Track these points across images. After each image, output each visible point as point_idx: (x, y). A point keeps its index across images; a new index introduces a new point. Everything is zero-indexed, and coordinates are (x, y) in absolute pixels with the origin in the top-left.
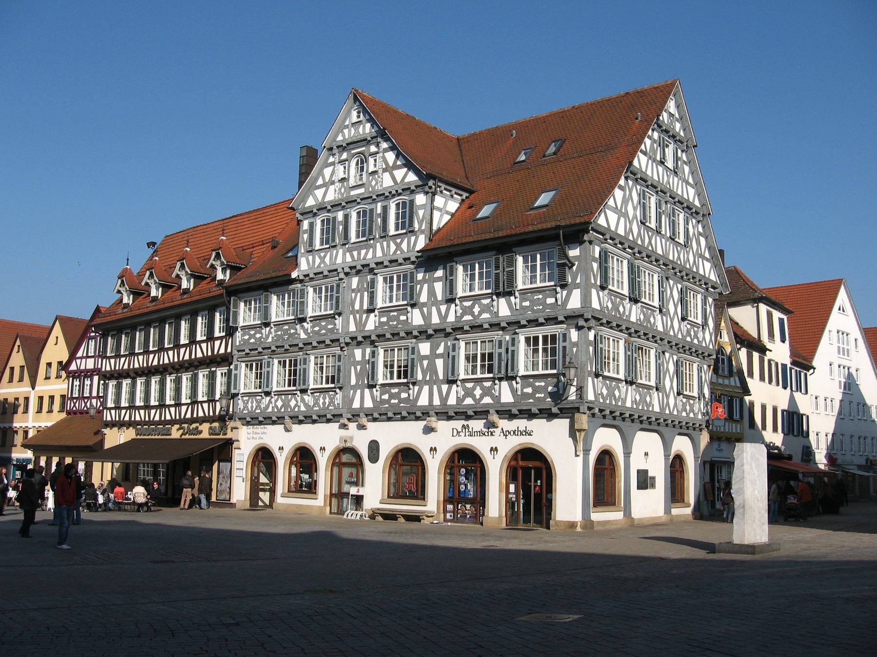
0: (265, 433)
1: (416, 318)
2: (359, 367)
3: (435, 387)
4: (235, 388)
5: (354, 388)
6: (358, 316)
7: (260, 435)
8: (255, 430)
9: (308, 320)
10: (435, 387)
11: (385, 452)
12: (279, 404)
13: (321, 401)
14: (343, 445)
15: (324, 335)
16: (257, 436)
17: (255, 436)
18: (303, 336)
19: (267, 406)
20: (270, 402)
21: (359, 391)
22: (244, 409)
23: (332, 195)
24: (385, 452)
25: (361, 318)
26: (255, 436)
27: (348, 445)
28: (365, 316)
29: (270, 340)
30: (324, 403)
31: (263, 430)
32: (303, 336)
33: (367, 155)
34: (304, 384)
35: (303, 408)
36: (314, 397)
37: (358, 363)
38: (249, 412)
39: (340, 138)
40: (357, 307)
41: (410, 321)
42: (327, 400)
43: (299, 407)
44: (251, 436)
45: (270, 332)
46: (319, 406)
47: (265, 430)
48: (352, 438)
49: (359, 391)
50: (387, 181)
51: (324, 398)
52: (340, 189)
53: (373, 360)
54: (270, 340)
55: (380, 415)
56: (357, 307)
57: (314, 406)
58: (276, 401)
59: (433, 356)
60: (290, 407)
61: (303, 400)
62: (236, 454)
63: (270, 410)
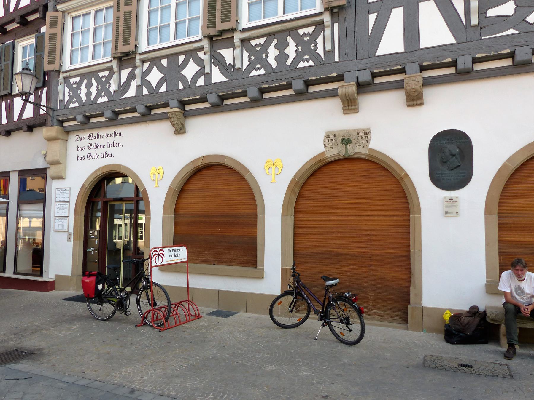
0: (115, 145)
4: (52, 61)
7: (109, 151)
8: (94, 142)
11: (488, 163)
12: (155, 76)
13: (273, 52)
14: (335, 152)
16: (100, 152)
17: (93, 152)
19: (126, 87)
20: (131, 77)
22: (70, 101)
24: (488, 163)
26: (93, 152)
27: (356, 149)
30: (282, 58)
31: (111, 140)
34: (226, 18)
35: (218, 77)
36: (251, 50)
38: (82, 105)
42: (291, 50)
43: (209, 76)
44: (84, 153)
46: (266, 65)
47: (117, 139)
48: (365, 135)
51: (282, 46)
55: (458, 67)
57: (251, 67)
58: (145, 74)
60: (184, 79)
61: (218, 61)
62: (54, 189)
63: (131, 92)
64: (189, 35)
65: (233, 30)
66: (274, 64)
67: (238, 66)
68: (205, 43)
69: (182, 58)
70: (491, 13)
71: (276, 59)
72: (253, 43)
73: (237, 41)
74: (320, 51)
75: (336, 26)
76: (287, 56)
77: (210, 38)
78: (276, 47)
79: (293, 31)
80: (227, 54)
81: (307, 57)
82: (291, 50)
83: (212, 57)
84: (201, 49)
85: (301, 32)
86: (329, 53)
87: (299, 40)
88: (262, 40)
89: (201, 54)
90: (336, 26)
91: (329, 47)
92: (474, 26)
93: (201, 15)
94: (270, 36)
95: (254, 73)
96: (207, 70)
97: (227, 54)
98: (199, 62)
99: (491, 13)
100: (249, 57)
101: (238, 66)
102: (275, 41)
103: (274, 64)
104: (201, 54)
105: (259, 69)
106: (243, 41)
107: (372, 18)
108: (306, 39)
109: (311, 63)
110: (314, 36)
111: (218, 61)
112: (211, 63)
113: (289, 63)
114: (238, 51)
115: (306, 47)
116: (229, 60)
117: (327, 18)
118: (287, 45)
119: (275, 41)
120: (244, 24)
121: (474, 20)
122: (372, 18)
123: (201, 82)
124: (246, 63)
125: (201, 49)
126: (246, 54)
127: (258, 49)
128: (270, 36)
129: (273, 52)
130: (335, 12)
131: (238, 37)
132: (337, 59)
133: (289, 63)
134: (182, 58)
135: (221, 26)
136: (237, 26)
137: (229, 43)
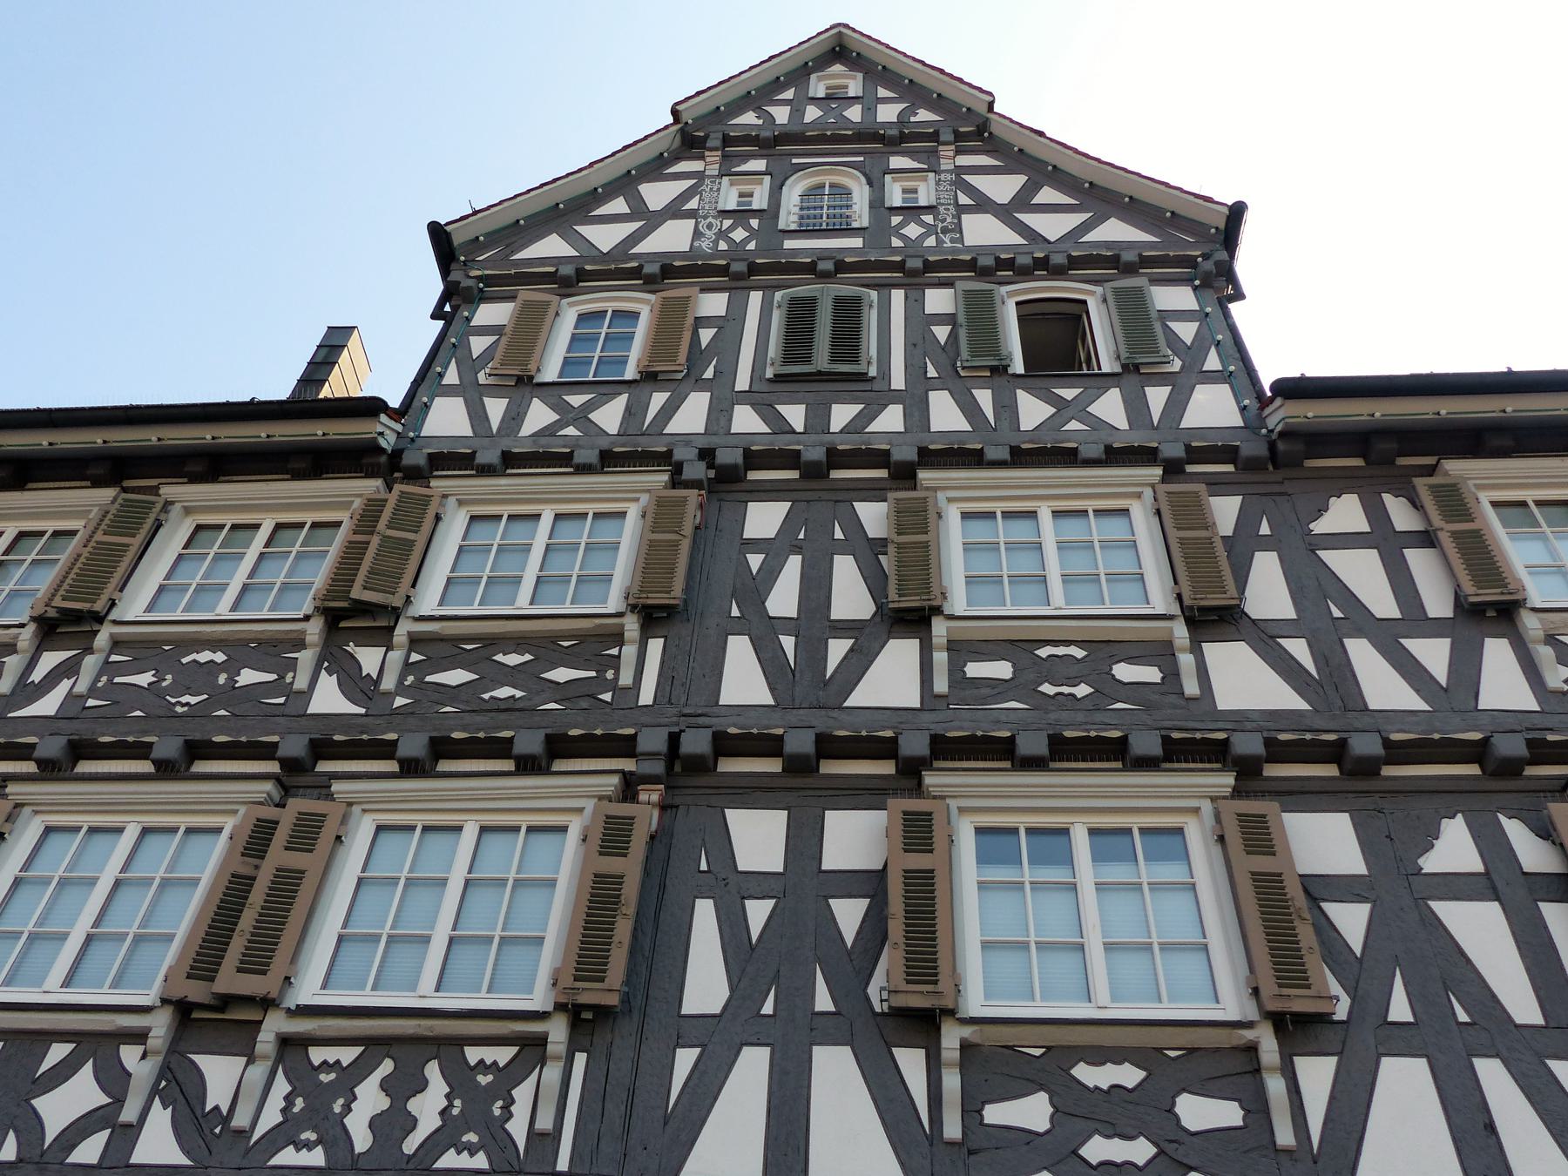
1: (1241, 681)
2: (758, 912)
3: (1492, 1075)
5: (720, 1040)
6: (788, 642)
9: (403, 630)
10: (1492, 1075)
13: (370, 1099)
15: (508, 706)
18: (329, 698)
21: (753, 1066)
23: (673, 238)
25: (813, 651)
28: (838, 649)
29: (48, 705)
30: (391, 1124)
32: (329, 698)
33: (876, 174)
34: (256, 962)
36: (303, 1078)
37: (759, 884)
39: (749, 118)
40: (783, 599)
41: (1191, 687)
42: (429, 1107)
43: (128, 1134)
45: (68, 670)
49: (753, 1066)
50: (983, 232)
51: (403, 1087)
52: (723, 234)
53: (918, 861)
54: (48, 705)
56: (783, 599)
57: (285, 1134)
59: (1398, 885)
61: (178, 1086)
64: (115, 984)
65: (267, 1003)
66: (362, 1140)
67: (240, 1120)
68: (160, 1025)
69: (58, 1052)
70: (995, 1114)
71: (374, 1124)
72: (317, 1055)
73: (266, 1039)
74: (518, 1129)
75: (581, 1059)
76: (413, 1123)
77: (183, 1010)
78: (385, 1085)
79: (448, 1048)
80: (220, 1075)
81: (471, 1137)
82: (429, 1107)
83: (166, 1071)
84: (139, 1037)
85: (473, 1054)
86: (543, 1141)
87: (460, 1078)
88: (347, 1055)
89: (130, 1055)
90: (581, 1059)
91: (545, 1122)
92: (952, 1144)
93: (181, 932)
94: (375, 1046)
95: (288, 1157)
96: (129, 1114)
97: (220, 1075)
98: (114, 1081)
99: (995, 1114)
100: (289, 1099)
101: (240, 1120)
102: (387, 1067)
103: (362, 1140)
104: (130, 1055)
105: (309, 1146)
106: (287, 1043)
107: (686, 1058)
108: (484, 1080)
109: (480, 1161)
110: (509, 1077)
111: (178, 1086)
112: (154, 1091)
113: (411, 1145)
114: (258, 1072)
115: (477, 1111)
116: (217, 1095)
117: (557, 1032)
118: (422, 1086)
119: (387, 1067)
120: (308, 991)
121: (952, 1129)
122: (686, 1058)
123: (89, 1151)
124: (271, 1116)
125: (139, 1037)
126: (281, 1087)
127: (325, 1078)
128: (375, 1046)
129: (370, 1099)
130: (586, 1021)
131: (274, 1025)
132: (563, 1164)
133: (411, 1145)
134: (58, 1052)
135: (229, 980)
136: (282, 992)
137: (240, 1039)
